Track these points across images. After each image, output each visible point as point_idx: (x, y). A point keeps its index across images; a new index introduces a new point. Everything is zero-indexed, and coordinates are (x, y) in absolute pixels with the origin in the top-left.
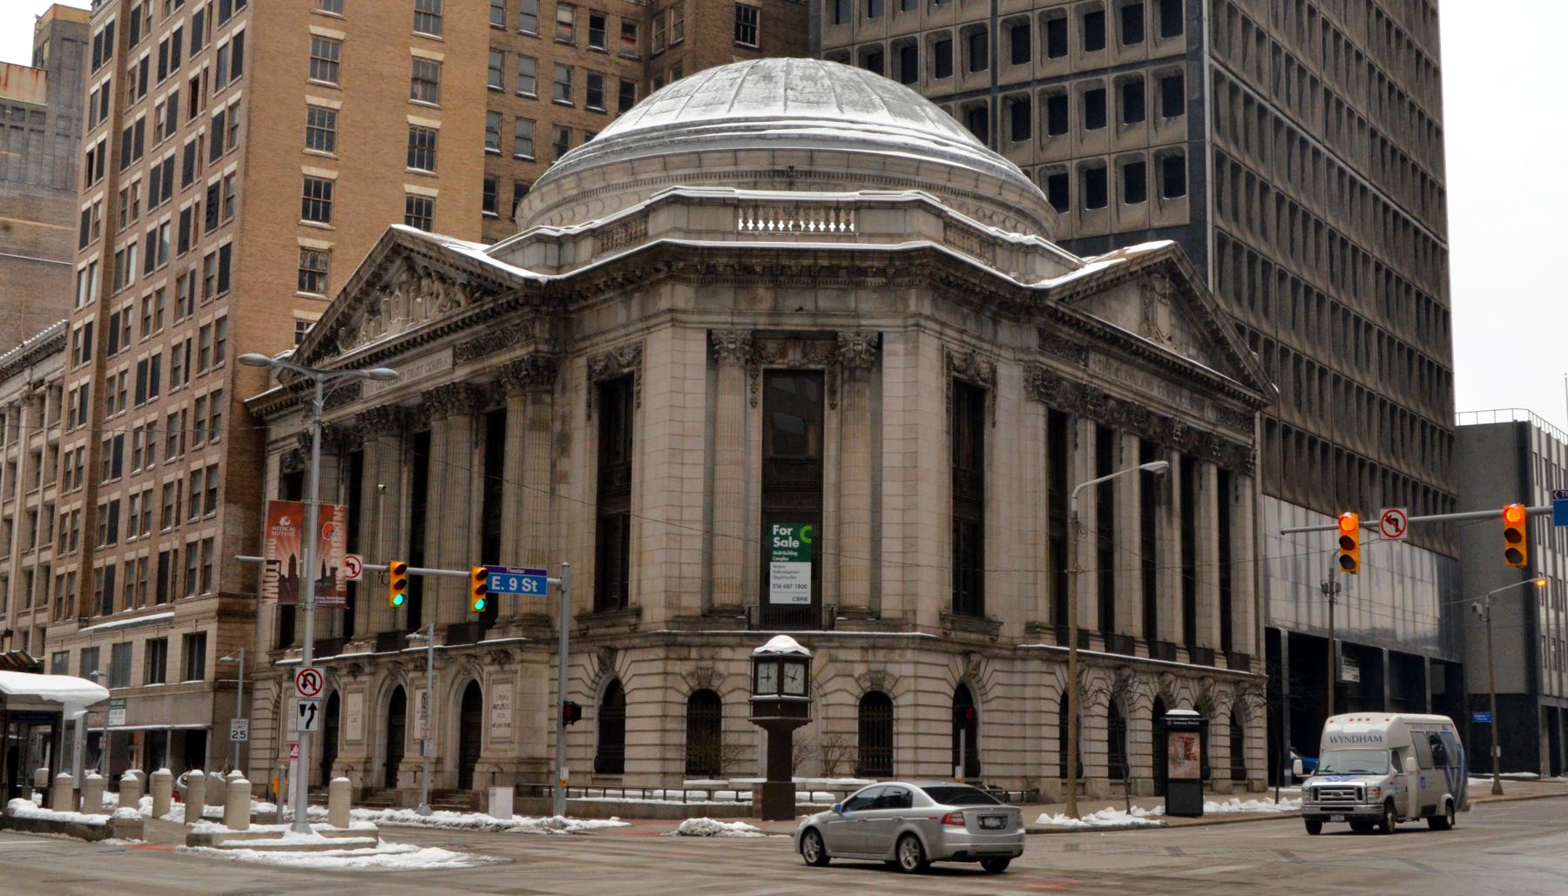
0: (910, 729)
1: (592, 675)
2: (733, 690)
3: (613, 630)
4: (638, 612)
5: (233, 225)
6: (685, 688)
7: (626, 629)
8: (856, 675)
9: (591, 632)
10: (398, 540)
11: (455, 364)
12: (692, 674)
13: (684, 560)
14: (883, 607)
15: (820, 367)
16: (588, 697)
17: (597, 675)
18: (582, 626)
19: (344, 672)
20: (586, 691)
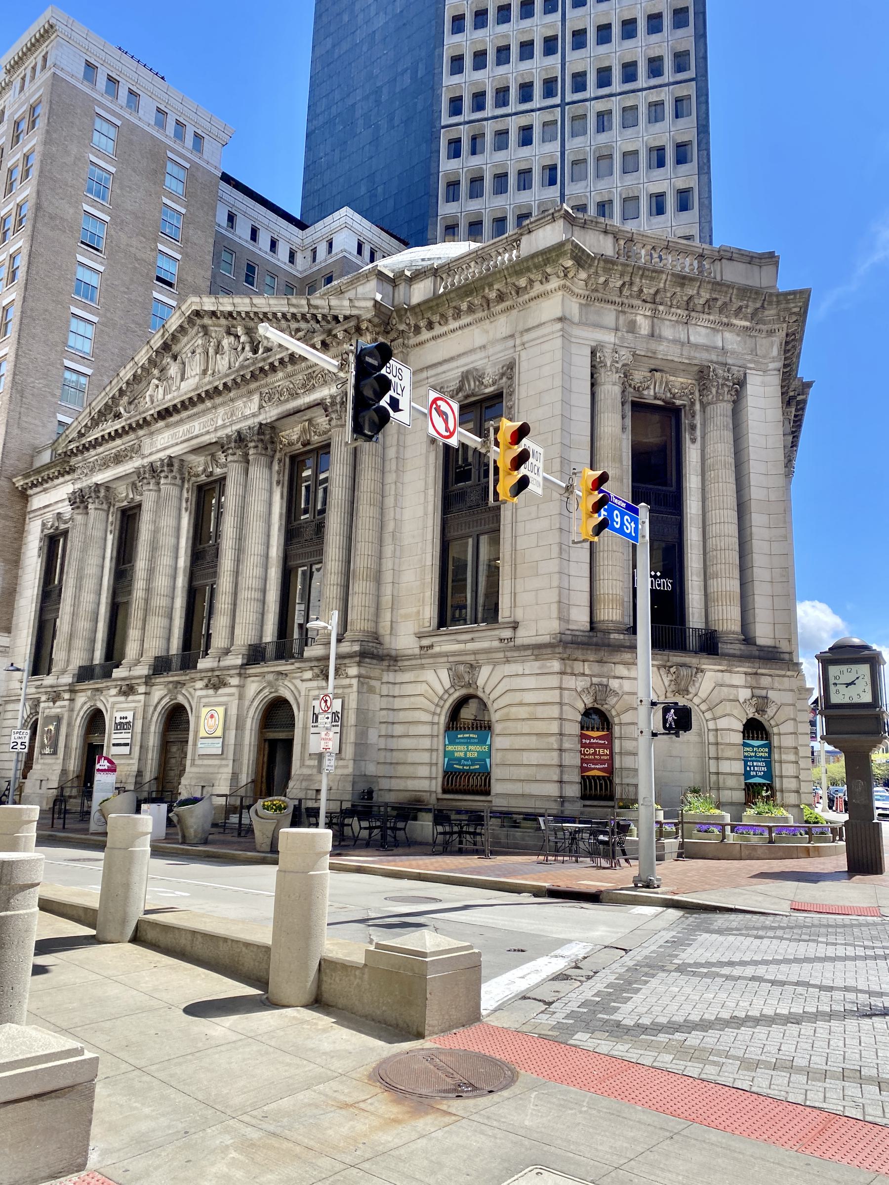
0: (792, 757)
1: (441, 692)
2: (627, 710)
3: (470, 646)
4: (515, 626)
5: (10, 340)
6: (581, 707)
7: (496, 644)
8: (742, 701)
9: (437, 649)
10: (174, 578)
11: (261, 407)
12: (586, 690)
13: (572, 573)
14: (757, 635)
15: (682, 402)
16: (434, 714)
17: (446, 691)
18: (426, 642)
19: (114, 691)
20: (432, 708)
